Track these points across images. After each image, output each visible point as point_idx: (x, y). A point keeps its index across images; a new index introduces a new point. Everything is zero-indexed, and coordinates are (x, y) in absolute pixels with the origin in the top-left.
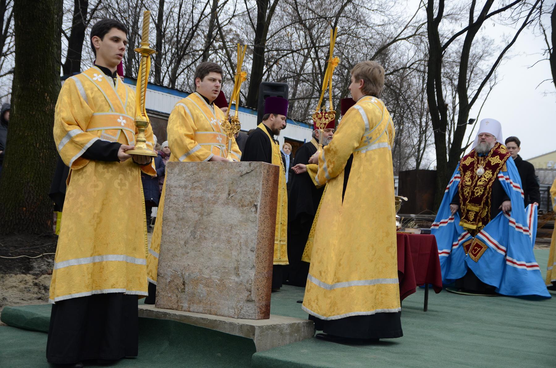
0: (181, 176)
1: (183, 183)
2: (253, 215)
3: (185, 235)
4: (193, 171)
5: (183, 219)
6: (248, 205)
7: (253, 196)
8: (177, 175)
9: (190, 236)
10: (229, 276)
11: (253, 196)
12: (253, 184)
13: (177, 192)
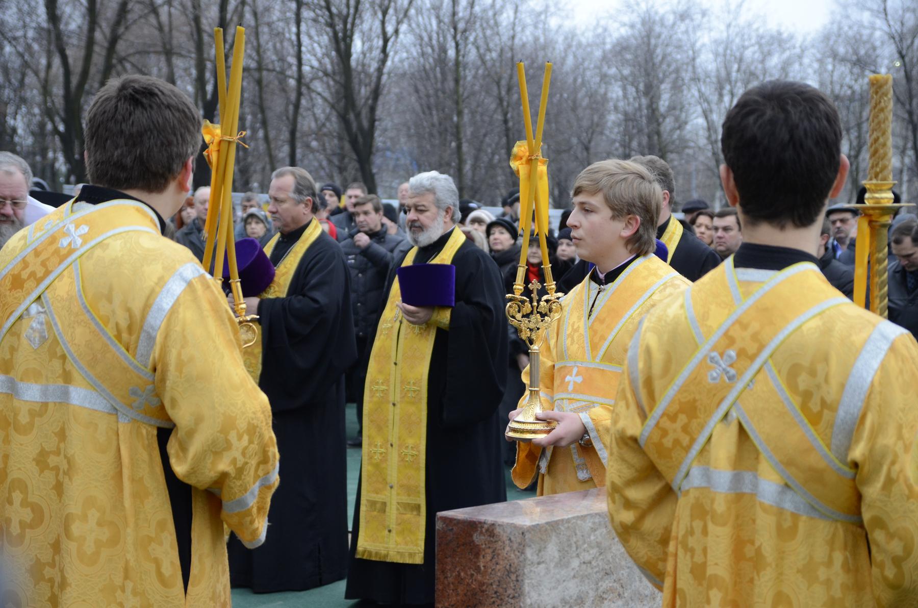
0: (567, 565)
4: (598, 545)
8: (556, 566)
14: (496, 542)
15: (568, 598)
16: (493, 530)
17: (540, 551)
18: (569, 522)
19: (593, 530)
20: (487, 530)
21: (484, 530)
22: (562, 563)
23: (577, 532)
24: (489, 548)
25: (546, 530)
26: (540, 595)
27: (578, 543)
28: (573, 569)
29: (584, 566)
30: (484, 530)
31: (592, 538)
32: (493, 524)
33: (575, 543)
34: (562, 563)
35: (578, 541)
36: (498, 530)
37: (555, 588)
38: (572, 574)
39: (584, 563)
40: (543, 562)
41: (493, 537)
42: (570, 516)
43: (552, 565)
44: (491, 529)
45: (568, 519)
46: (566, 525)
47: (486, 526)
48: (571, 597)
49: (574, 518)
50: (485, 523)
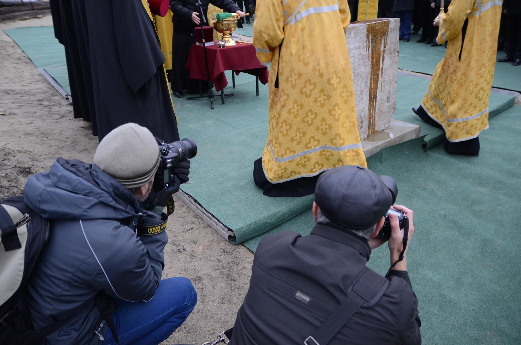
0: (356, 38)
1: (357, 44)
2: (397, 58)
3: (360, 87)
5: (358, 74)
6: (393, 52)
7: (395, 45)
8: (353, 38)
9: (364, 86)
10: (384, 104)
11: (395, 45)
12: (395, 36)
13: (353, 54)
15: (356, 47)
17: (349, 34)
19: (363, 29)
22: (355, 38)
25: (351, 29)
26: (349, 46)
28: (358, 39)
29: (360, 39)
31: (363, 31)
34: (355, 38)
37: (353, 44)
38: (357, 41)
39: (361, 38)
40: (350, 37)
43: (352, 38)
48: (357, 47)
49: (358, 26)
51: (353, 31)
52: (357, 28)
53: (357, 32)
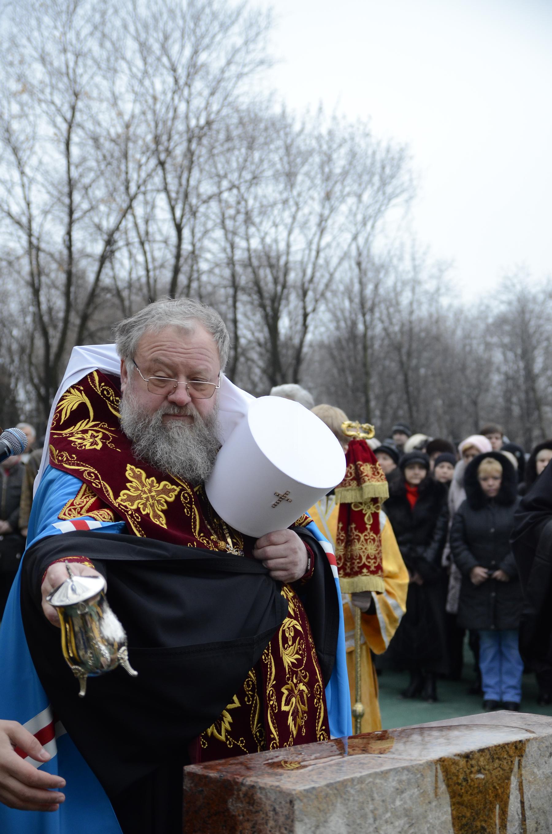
14: (257, 812)
16: (253, 794)
18: (362, 783)
20: (246, 795)
21: (241, 795)
23: (375, 795)
24: (248, 820)
27: (376, 812)
30: (241, 795)
32: (253, 787)
33: (372, 812)
35: (376, 809)
36: (259, 795)
41: (253, 805)
42: (365, 773)
44: (250, 793)
45: (361, 777)
46: (358, 787)
47: (244, 789)
49: (369, 775)
50: (242, 784)
51: (340, 807)
52: (361, 791)
53: (362, 808)
